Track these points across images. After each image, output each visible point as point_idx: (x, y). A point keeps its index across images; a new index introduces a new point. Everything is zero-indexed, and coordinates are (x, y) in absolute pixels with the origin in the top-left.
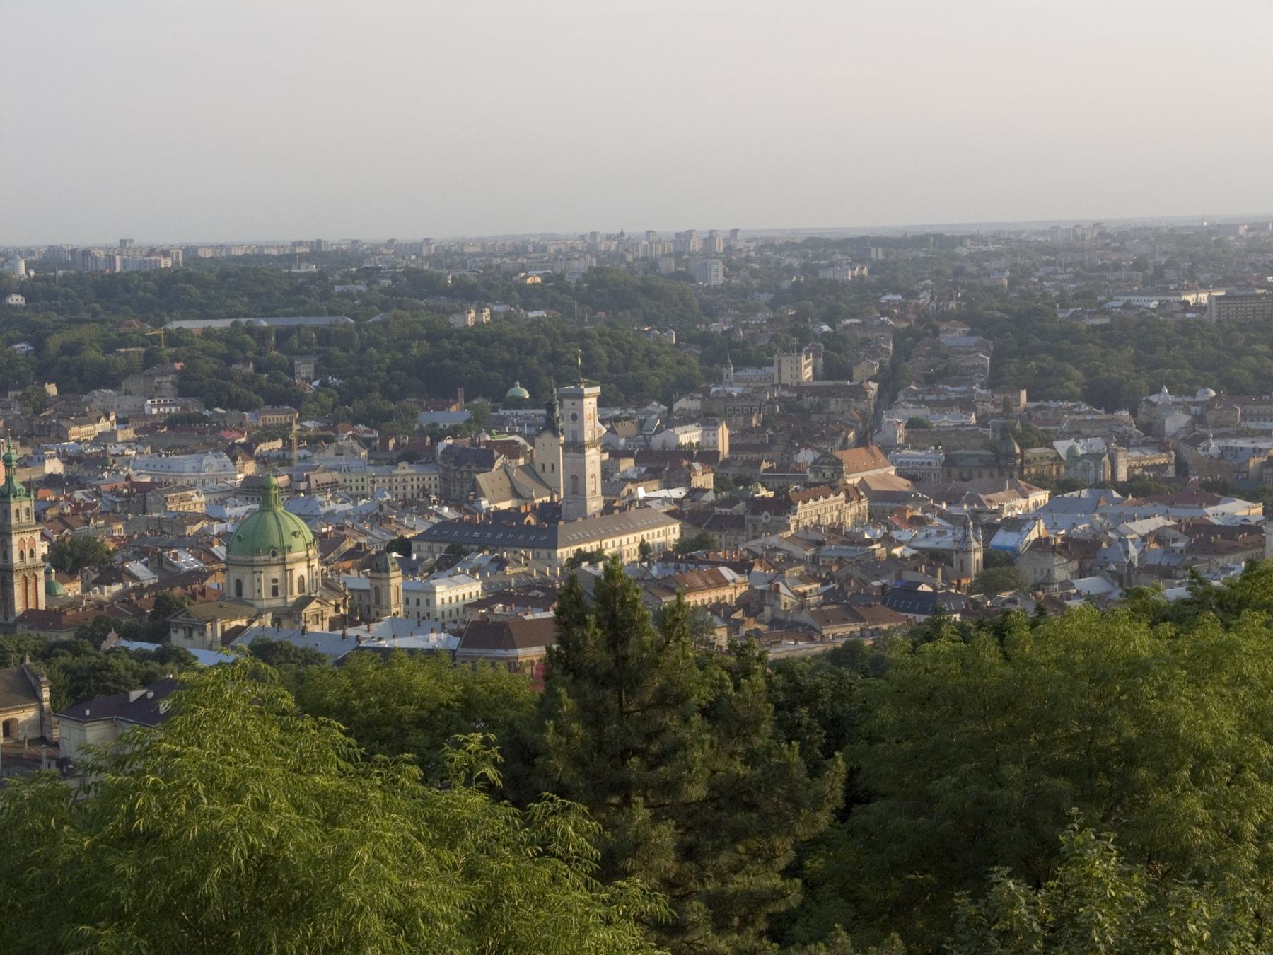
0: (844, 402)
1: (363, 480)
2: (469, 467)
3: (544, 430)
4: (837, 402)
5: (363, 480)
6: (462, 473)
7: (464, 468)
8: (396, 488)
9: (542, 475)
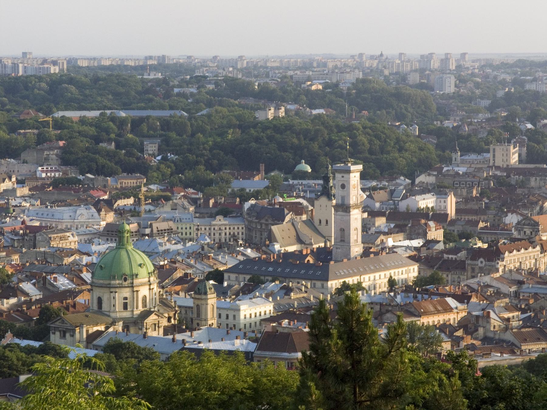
0: (541, 180)
1: (190, 228)
2: (267, 220)
3: (321, 195)
4: (536, 179)
5: (190, 228)
6: (261, 224)
7: (263, 221)
8: (214, 234)
9: (319, 228)
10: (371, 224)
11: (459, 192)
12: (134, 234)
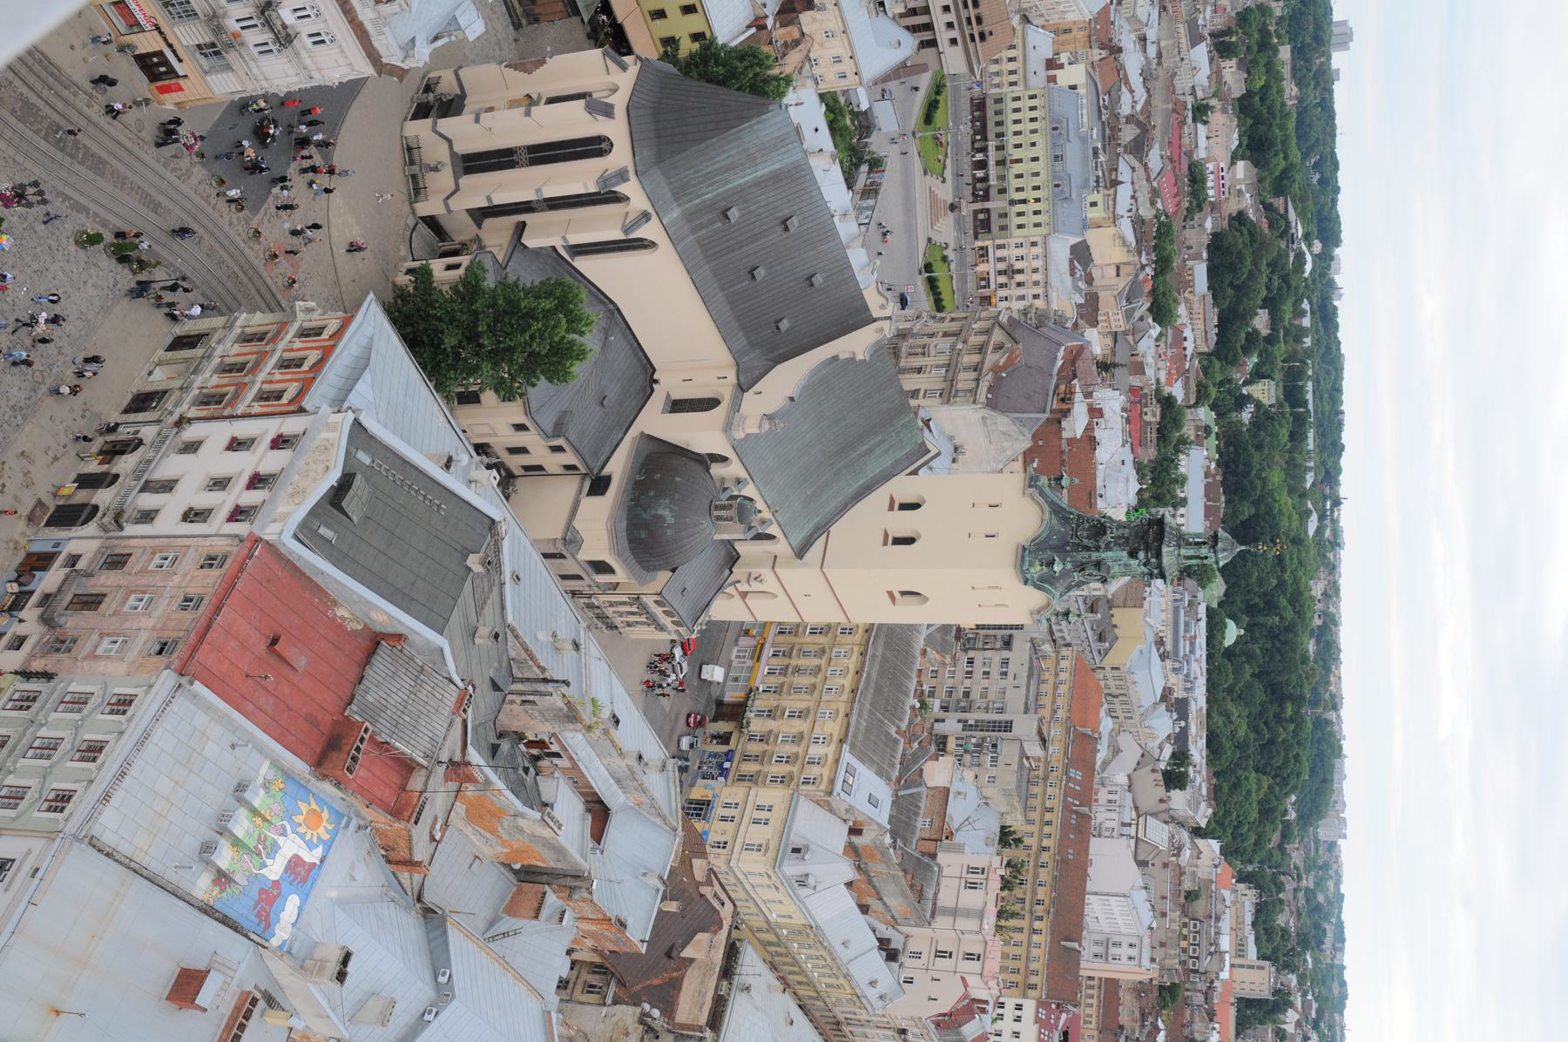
1: (1037, 225)
2: (999, 347)
3: (1057, 510)
5: (1037, 225)
6: (988, 332)
7: (998, 336)
8: (1022, 298)
10: (993, 772)
11: (1173, 952)
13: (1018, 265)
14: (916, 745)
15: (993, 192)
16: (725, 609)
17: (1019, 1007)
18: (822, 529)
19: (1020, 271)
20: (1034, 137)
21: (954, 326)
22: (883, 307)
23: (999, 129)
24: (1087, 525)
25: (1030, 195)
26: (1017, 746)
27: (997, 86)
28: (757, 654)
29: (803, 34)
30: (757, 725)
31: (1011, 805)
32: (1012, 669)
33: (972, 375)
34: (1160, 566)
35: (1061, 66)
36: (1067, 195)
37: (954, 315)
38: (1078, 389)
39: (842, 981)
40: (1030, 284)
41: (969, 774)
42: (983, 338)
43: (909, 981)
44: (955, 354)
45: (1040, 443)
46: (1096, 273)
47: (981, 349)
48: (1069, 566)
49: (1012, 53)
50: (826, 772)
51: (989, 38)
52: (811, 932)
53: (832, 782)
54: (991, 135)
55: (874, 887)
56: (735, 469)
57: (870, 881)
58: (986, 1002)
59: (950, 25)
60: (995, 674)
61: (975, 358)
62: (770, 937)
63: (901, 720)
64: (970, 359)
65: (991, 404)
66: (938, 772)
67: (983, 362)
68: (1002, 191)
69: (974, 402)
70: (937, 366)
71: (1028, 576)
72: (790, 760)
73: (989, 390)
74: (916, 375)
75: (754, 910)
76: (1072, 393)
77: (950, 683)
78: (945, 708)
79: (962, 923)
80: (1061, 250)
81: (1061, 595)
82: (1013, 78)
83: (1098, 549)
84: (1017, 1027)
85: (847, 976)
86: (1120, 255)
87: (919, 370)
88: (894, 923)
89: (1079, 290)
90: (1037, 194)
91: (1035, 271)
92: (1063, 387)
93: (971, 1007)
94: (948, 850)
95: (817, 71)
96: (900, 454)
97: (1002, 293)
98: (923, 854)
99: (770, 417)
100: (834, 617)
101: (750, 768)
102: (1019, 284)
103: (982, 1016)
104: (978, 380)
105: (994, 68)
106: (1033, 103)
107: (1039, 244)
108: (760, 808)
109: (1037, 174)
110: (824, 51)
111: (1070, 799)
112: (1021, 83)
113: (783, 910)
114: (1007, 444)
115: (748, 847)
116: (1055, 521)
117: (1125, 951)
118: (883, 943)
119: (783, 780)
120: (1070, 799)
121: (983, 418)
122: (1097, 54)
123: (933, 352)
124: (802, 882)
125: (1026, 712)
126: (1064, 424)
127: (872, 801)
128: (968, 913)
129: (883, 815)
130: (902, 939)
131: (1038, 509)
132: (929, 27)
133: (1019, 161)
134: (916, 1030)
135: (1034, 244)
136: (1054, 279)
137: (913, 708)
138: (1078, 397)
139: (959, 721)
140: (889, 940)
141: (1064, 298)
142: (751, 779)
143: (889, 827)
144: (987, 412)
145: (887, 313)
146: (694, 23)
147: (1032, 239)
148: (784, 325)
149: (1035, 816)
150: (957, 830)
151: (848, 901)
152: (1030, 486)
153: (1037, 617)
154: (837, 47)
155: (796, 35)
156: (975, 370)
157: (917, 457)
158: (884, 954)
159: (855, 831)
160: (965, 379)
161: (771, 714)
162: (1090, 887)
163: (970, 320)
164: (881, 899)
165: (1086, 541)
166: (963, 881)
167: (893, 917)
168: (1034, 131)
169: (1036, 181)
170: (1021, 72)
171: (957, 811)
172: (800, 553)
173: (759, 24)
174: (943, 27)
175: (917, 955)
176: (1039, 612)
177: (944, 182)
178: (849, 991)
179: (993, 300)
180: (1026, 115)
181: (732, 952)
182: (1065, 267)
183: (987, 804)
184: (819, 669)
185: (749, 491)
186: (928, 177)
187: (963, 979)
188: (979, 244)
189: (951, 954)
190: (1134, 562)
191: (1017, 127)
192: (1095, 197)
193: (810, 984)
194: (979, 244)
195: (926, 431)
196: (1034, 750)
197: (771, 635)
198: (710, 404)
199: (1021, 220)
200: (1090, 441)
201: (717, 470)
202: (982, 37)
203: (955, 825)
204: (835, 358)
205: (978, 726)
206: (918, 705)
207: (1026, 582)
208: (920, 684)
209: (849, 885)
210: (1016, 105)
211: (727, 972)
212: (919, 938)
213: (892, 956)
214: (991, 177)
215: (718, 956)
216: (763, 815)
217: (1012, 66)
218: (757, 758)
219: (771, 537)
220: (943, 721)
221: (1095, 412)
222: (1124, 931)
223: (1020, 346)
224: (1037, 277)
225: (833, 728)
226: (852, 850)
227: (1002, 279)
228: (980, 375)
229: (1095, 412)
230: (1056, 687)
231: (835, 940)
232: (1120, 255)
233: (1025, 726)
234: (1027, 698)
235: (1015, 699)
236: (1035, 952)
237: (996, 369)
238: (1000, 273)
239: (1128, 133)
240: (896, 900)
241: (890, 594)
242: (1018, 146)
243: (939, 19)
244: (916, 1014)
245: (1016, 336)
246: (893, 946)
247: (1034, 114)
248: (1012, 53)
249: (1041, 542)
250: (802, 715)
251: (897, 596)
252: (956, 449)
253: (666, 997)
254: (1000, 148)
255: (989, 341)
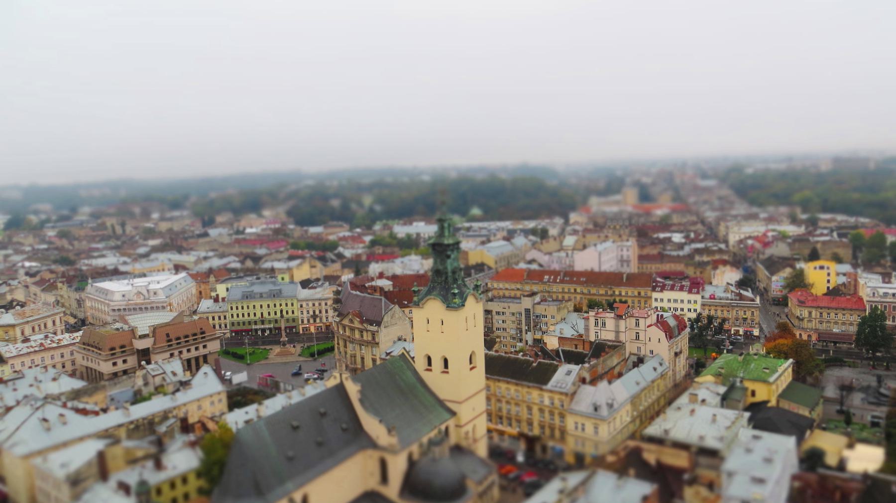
1: (292, 305)
2: (351, 321)
3: (429, 293)
5: (292, 305)
6: (344, 327)
7: (346, 322)
8: (327, 311)
10: (549, 317)
12: (118, 350)
13: (311, 313)
14: (540, 353)
15: (277, 325)
16: (482, 450)
17: (656, 300)
18: (441, 403)
19: (314, 312)
20: (251, 307)
21: (341, 343)
22: (335, 378)
23: (247, 324)
24: (436, 278)
25: (278, 309)
26: (536, 306)
27: (226, 326)
28: (501, 433)
29: (199, 422)
30: (536, 431)
31: (564, 308)
32: (501, 310)
33: (365, 334)
34: (453, 245)
35: (217, 295)
36: (278, 291)
37: (336, 342)
38: (370, 284)
39: (655, 384)
40: (320, 307)
41: (552, 328)
42: (347, 329)
43: (652, 352)
44: (353, 341)
45: (396, 300)
46: (314, 277)
47: (352, 329)
48: (455, 286)
49: (211, 319)
50: (557, 397)
51: (204, 329)
52: (634, 400)
53: (561, 393)
54: (249, 327)
55: (609, 371)
56: (415, 449)
57: (606, 373)
58: (658, 315)
59: (197, 349)
60: (503, 318)
61: (357, 332)
62: (638, 422)
63: (529, 361)
64: (357, 335)
65: (379, 324)
66: (552, 343)
67: (358, 328)
68: (276, 321)
69: (378, 332)
70: (361, 350)
71: (461, 304)
72: (552, 413)
73: (371, 325)
74: (365, 360)
75: (626, 430)
76: (372, 286)
77: (509, 338)
78: (521, 340)
79: (622, 328)
80: (305, 293)
81: (469, 289)
82: (222, 318)
83: (447, 273)
84: (665, 300)
85: (653, 382)
86: (306, 267)
87: (363, 358)
88: (626, 360)
89: (323, 284)
90: (278, 305)
91: (314, 305)
92: (369, 291)
93: (661, 323)
94: (588, 336)
95: (217, 414)
96: (405, 367)
97: (324, 320)
98: (590, 349)
99: (390, 431)
100: (483, 396)
101: (557, 433)
102: (320, 312)
103: (664, 317)
104: (367, 331)
105: (217, 327)
106: (234, 308)
107: (301, 303)
108: (576, 428)
109: (269, 306)
110: (209, 410)
111: (558, 281)
112: (225, 314)
113: (624, 415)
114: (397, 316)
115: (596, 433)
116: (434, 293)
117: (625, 253)
118: (636, 365)
119: (562, 416)
120: (558, 281)
121: (385, 327)
122: (212, 279)
123: (354, 352)
124: (610, 406)
125: (521, 303)
126: (386, 290)
127: (569, 373)
128: (617, 326)
129: (575, 368)
130: (632, 357)
131: (429, 301)
132: (197, 359)
133: (262, 314)
134: (675, 348)
135: (301, 306)
136: (318, 296)
137: (523, 356)
138: (374, 283)
139: (526, 333)
140: (634, 362)
141: (326, 292)
142: (563, 432)
143: (580, 365)
144: (382, 326)
145: (338, 375)
146: (192, 479)
147: (299, 307)
148: (344, 426)
149: (566, 296)
150: (578, 332)
151: (618, 383)
152: (418, 305)
153: (479, 299)
154: (206, 405)
155: (199, 425)
156: (362, 332)
157: (405, 359)
158: (640, 365)
159: (583, 381)
160: (367, 337)
161: (530, 423)
162: (596, 269)
163: (338, 335)
164: (614, 367)
165: (443, 278)
166: (602, 329)
167: (622, 361)
168: (248, 307)
169: (272, 305)
170: (219, 314)
171: (569, 333)
172: (453, 414)
173: (193, 445)
174: (198, 352)
175: (639, 349)
176: (476, 299)
177: (271, 349)
178: (659, 381)
179: (328, 324)
180: (240, 311)
181: (652, 440)
182: (312, 291)
183: (564, 319)
184: (508, 403)
185: (425, 440)
186: (270, 357)
187: (648, 327)
188: (301, 332)
189: (637, 333)
190: (453, 256)
191: (246, 315)
192: (279, 277)
193: (658, 400)
194: (301, 332)
195: (392, 354)
196: (537, 299)
197: (492, 426)
198: (383, 465)
199: (290, 312)
200: (394, 278)
201: (416, 456)
202: (203, 333)
203: (575, 333)
204: (361, 401)
205: (528, 324)
206: (522, 353)
207: (463, 305)
208: (511, 353)
209: (610, 382)
210: (235, 316)
211: (658, 441)
212: (631, 348)
213: (640, 361)
214: (269, 327)
215: (652, 447)
216: (580, 426)
217: (216, 318)
218: (552, 429)
219: (447, 429)
220: (527, 341)
221: (381, 276)
222: (614, 254)
223: (351, 311)
224: (317, 304)
225: (535, 394)
226: (594, 382)
227: (318, 320)
228: (364, 330)
229: (381, 276)
230: (507, 289)
231: (636, 389)
232: (306, 267)
233: (527, 303)
234: (513, 302)
235: (514, 307)
236: (630, 294)
237: (362, 322)
238: (315, 321)
239: (249, 264)
240: (615, 361)
241: (472, 369)
242: (255, 314)
243: (194, 353)
244: (667, 348)
245: (345, 313)
246: (636, 360)
247: (240, 308)
248: (211, 319)
249: (445, 299)
250: (530, 409)
251: (472, 366)
252: (400, 339)
253: (678, 472)
254: (256, 323)
255: (348, 326)
